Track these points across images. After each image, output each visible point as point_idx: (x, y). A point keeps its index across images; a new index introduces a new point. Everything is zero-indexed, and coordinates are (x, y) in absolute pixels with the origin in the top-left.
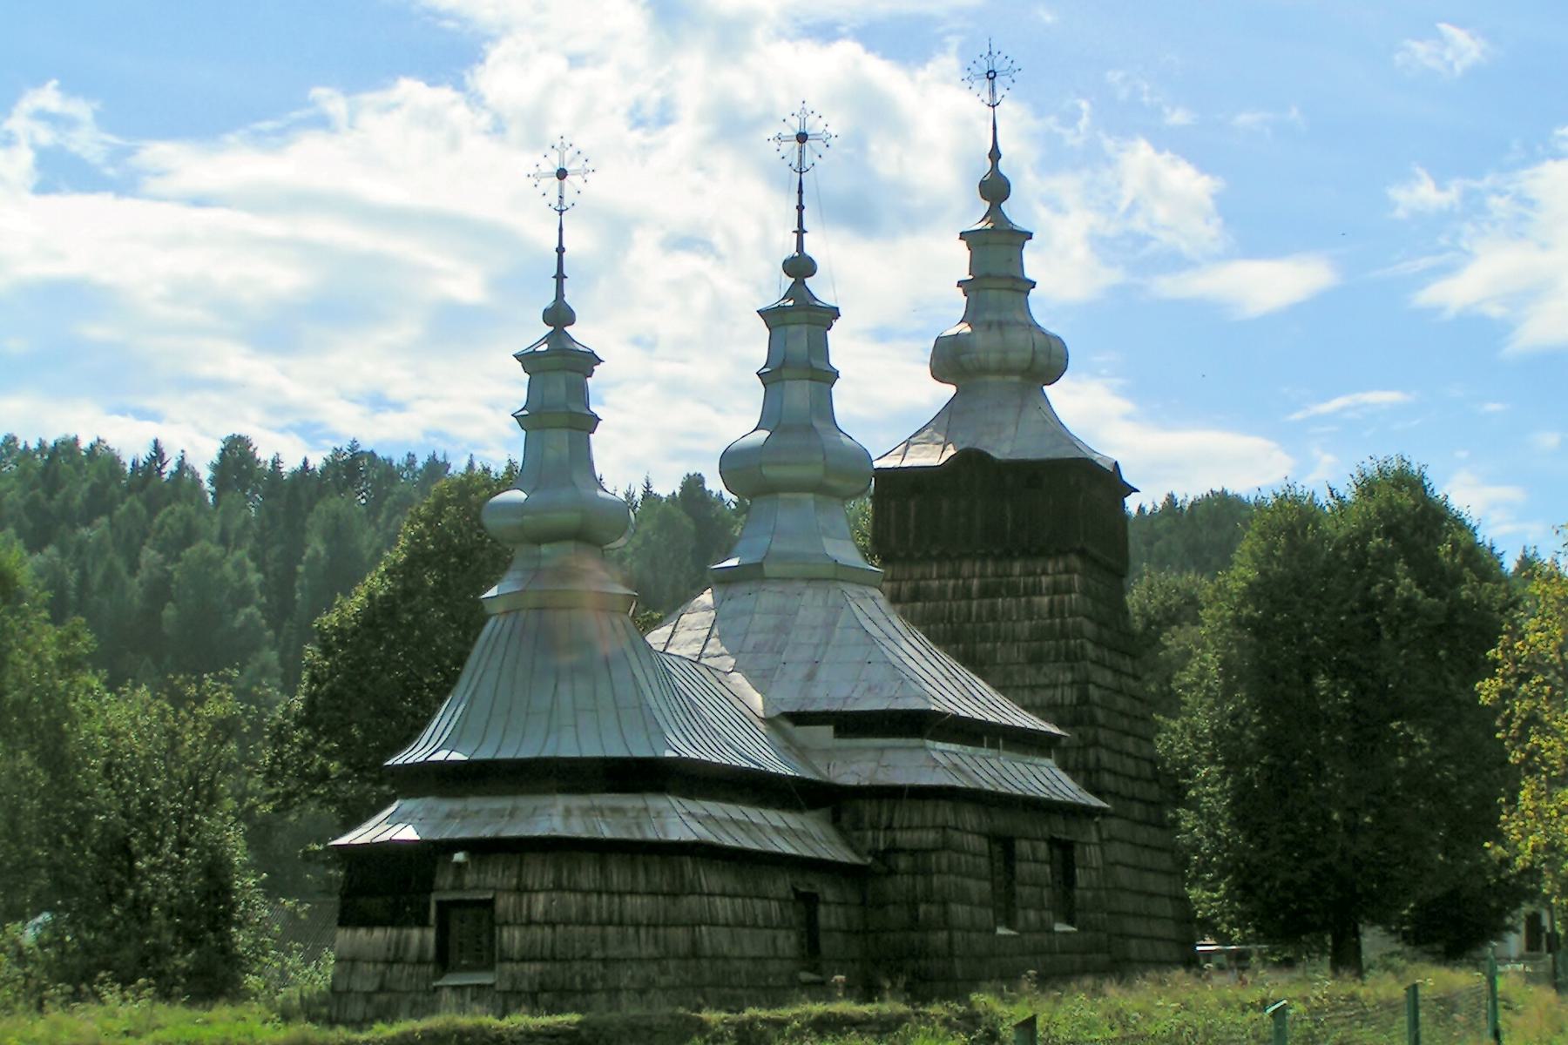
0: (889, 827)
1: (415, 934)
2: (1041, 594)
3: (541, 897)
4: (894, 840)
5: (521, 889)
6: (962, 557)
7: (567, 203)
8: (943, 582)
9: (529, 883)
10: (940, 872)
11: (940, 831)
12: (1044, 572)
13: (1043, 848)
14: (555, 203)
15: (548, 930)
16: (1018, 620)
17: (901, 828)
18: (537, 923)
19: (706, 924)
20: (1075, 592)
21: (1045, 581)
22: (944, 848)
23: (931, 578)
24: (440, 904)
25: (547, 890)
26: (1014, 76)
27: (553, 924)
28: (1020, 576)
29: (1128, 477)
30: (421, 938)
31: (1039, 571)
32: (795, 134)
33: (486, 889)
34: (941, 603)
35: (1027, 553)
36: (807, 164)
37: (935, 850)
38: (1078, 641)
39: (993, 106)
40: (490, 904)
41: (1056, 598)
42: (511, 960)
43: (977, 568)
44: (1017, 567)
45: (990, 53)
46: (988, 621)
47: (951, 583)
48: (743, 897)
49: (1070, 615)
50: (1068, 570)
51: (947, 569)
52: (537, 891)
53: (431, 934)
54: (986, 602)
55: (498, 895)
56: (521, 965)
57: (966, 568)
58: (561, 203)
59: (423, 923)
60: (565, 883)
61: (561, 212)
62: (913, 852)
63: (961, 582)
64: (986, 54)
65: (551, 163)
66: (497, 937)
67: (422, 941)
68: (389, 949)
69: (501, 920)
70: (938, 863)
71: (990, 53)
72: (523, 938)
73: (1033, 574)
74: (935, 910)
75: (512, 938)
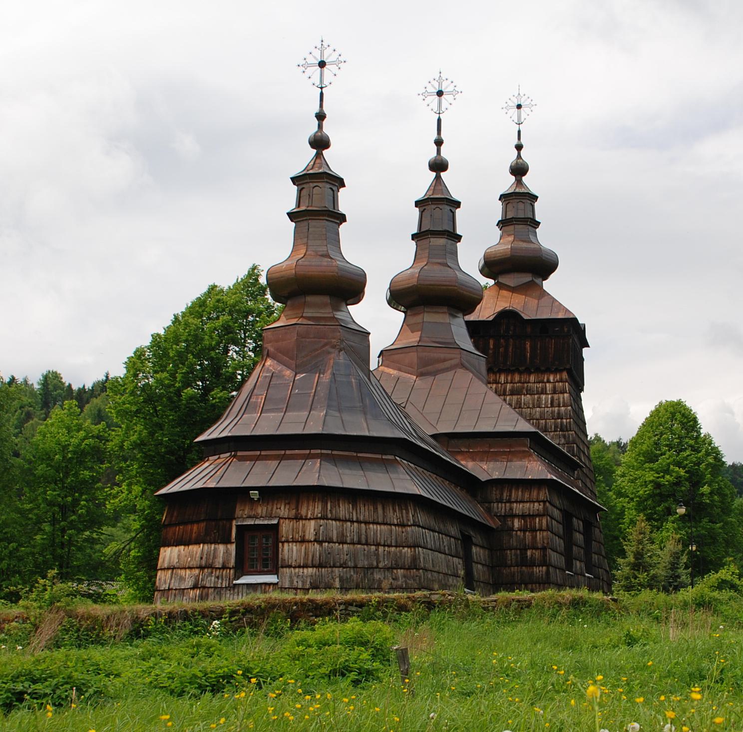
0: (510, 501)
1: (221, 548)
2: (546, 394)
3: (313, 522)
4: (511, 509)
5: (298, 518)
9: (303, 512)
10: (541, 530)
11: (542, 504)
12: (548, 381)
15: (317, 546)
16: (534, 407)
17: (516, 502)
19: (421, 547)
20: (566, 393)
22: (543, 515)
24: (237, 526)
26: (532, 108)
27: (320, 543)
28: (534, 383)
29: (589, 336)
30: (225, 552)
31: (545, 380)
32: (436, 91)
33: (271, 517)
35: (538, 370)
36: (443, 109)
38: (568, 420)
39: (519, 124)
40: (276, 527)
41: (556, 396)
42: (290, 566)
43: (509, 378)
44: (532, 378)
48: (439, 533)
49: (563, 406)
50: (561, 381)
52: (310, 519)
53: (233, 548)
54: (515, 397)
55: (282, 521)
56: (297, 570)
57: (502, 379)
59: (226, 541)
60: (329, 516)
62: (523, 516)
63: (500, 385)
66: (280, 550)
67: (227, 552)
68: (201, 558)
69: (283, 539)
72: (299, 551)
73: (543, 382)
74: (537, 553)
75: (290, 551)
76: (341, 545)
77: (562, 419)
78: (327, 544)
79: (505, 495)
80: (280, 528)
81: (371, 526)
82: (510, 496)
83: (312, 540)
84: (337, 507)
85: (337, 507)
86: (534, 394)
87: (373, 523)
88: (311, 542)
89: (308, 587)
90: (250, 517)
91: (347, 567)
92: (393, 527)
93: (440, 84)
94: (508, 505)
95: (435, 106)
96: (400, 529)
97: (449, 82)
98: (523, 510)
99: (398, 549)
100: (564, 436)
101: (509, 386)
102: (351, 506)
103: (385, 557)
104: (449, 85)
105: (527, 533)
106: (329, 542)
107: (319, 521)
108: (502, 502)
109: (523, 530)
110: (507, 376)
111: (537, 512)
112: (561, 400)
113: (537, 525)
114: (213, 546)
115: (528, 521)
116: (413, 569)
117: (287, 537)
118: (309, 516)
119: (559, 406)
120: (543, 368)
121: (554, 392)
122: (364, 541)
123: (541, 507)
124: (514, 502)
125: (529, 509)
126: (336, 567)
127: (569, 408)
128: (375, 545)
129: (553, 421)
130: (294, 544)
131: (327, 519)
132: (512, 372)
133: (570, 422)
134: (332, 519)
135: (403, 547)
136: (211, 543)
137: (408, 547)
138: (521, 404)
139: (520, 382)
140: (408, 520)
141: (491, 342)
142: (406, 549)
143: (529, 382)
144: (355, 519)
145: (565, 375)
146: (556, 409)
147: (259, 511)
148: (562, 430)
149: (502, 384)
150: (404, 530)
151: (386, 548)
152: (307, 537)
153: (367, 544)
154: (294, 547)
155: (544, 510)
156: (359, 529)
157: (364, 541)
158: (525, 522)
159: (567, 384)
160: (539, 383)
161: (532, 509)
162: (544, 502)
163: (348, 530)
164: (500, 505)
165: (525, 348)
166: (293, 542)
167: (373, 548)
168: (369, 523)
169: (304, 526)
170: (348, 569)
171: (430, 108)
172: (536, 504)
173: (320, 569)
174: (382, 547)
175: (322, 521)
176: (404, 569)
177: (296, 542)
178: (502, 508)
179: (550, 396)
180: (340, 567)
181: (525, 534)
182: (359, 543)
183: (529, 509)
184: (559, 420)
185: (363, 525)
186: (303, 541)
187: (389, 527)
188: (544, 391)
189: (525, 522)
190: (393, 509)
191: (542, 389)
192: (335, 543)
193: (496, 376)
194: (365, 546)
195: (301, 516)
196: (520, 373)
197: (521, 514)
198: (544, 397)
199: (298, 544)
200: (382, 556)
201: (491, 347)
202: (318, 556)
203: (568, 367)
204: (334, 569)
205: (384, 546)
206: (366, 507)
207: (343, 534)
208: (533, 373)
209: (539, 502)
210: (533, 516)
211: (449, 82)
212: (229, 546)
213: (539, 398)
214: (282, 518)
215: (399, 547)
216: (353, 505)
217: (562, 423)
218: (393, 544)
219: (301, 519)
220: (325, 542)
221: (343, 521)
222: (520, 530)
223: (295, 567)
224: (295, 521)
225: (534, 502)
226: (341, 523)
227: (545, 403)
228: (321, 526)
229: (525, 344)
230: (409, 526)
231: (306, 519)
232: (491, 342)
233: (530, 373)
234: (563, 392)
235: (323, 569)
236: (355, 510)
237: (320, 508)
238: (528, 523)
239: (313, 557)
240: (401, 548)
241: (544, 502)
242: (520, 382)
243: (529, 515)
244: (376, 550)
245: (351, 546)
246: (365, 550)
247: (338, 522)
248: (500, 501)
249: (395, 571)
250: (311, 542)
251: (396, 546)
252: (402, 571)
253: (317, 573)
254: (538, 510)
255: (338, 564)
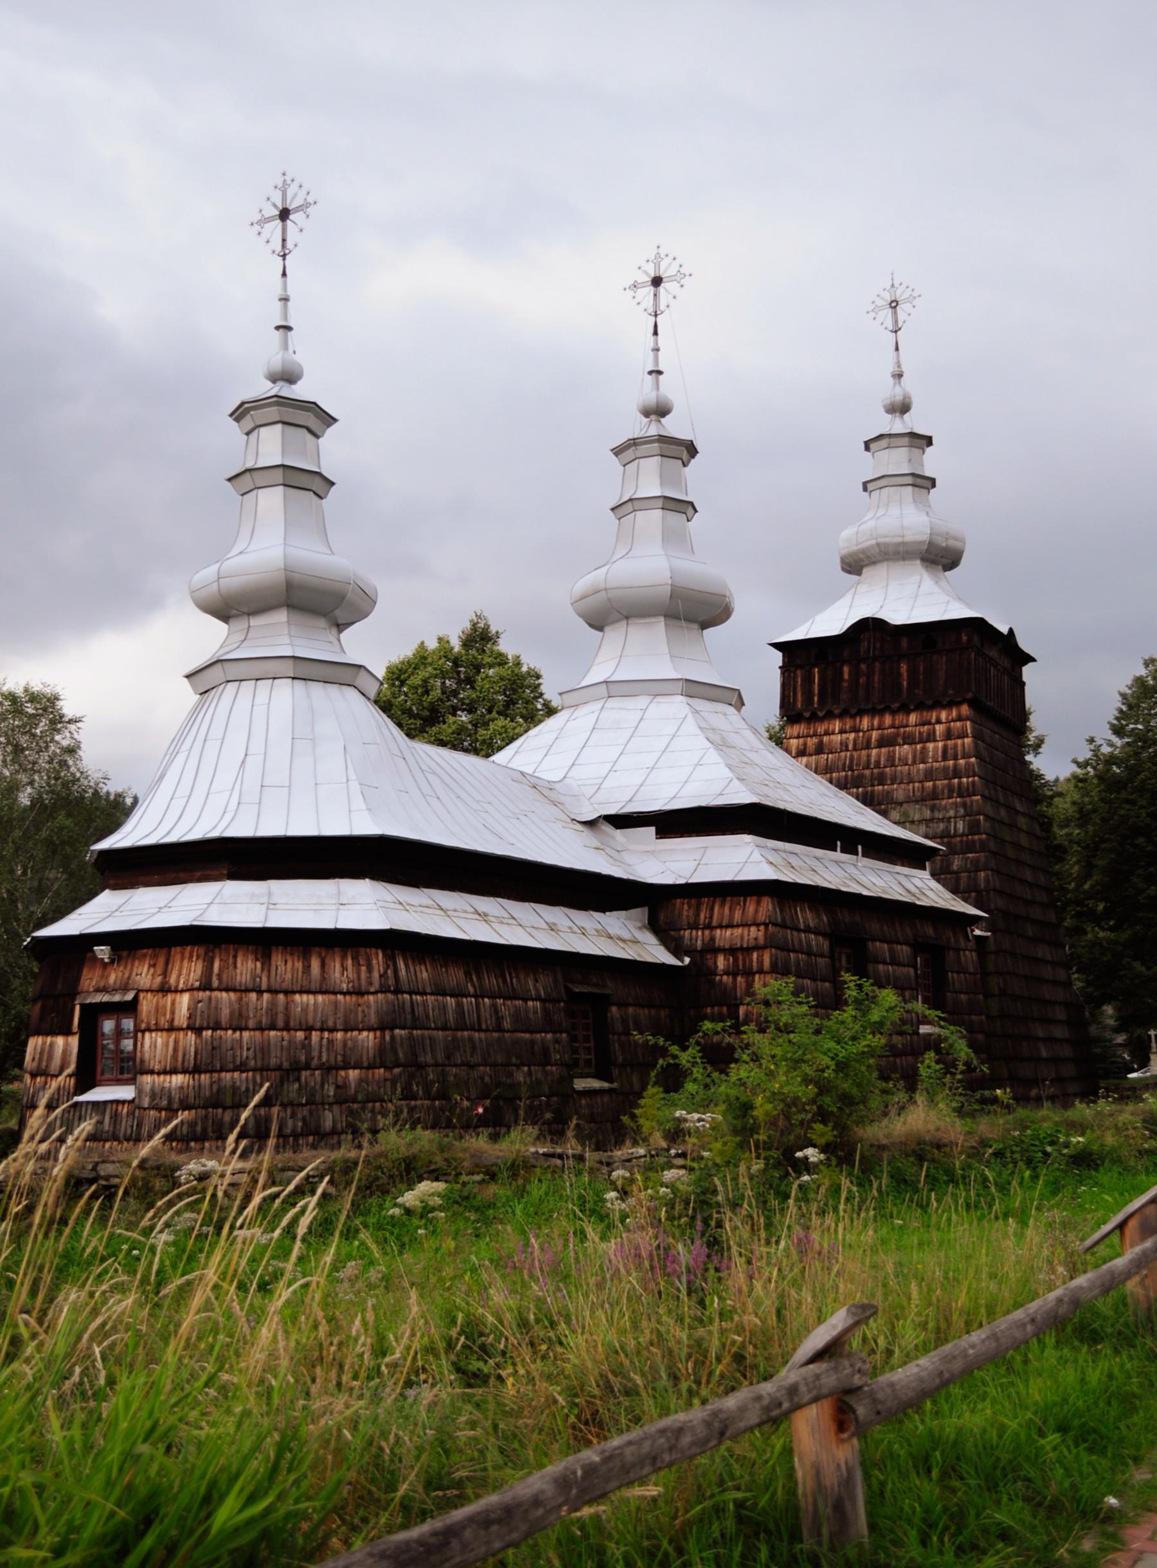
0: (709, 927)
1: (60, 1041)
2: (935, 741)
3: (185, 998)
4: (713, 939)
5: (164, 989)
6: (861, 713)
7: (289, 245)
8: (844, 736)
10: (761, 971)
11: (762, 928)
12: (939, 722)
13: (904, 950)
14: (279, 248)
15: (191, 1036)
16: (914, 763)
17: (721, 927)
18: (181, 1029)
21: (939, 728)
22: (764, 948)
23: (833, 733)
24: (84, 1007)
25: (191, 990)
27: (198, 1031)
31: (933, 720)
32: (649, 279)
34: (843, 754)
35: (920, 707)
36: (662, 307)
37: (757, 948)
42: (152, 1072)
43: (876, 722)
44: (913, 718)
45: (893, 286)
46: (885, 767)
47: (852, 736)
49: (963, 758)
50: (960, 718)
51: (849, 724)
52: (182, 991)
53: (74, 1041)
54: (884, 750)
55: (142, 995)
56: (162, 1077)
57: (865, 723)
58: (284, 246)
59: (67, 1032)
61: (284, 256)
62: (732, 951)
63: (861, 734)
64: (888, 287)
65: (275, 206)
70: (760, 962)
71: (893, 286)
73: (929, 723)
76: (238, 1033)
77: (960, 778)
78: (209, 1032)
79: (702, 916)
80: (139, 1007)
81: (297, 997)
82: (711, 917)
83: (185, 1026)
84: (231, 968)
85: (231, 968)
86: (916, 743)
87: (301, 992)
88: (182, 1029)
89: (175, 1106)
90: (98, 990)
91: (248, 1071)
92: (340, 997)
93: (657, 266)
94: (707, 932)
95: (649, 302)
96: (354, 998)
97: (669, 259)
98: (731, 940)
99: (349, 1034)
100: (964, 805)
101: (875, 735)
102: (259, 964)
103: (324, 1049)
104: (670, 264)
105: (739, 979)
106: (214, 1029)
107: (195, 993)
108: (697, 929)
109: (733, 973)
110: (873, 719)
111: (752, 943)
112: (960, 748)
113: (755, 964)
114: (49, 1039)
115: (741, 957)
116: (379, 1068)
117: (148, 1023)
118: (181, 986)
119: (955, 758)
120: (929, 702)
121: (948, 735)
122: (280, 1023)
123: (761, 934)
124: (716, 928)
125: (742, 937)
126: (227, 1071)
127: (973, 760)
128: (305, 1030)
129: (946, 782)
130: (159, 1034)
131: (212, 990)
132: (881, 712)
133: (973, 782)
134: (220, 990)
135: (360, 1030)
136: (47, 1034)
137: (369, 1030)
138: (894, 760)
139: (893, 726)
140: (371, 984)
141: (846, 669)
142: (365, 1034)
143: (907, 726)
144: (264, 987)
145: (965, 709)
146: (951, 762)
147: (112, 978)
148: (960, 795)
149: (864, 732)
150: (361, 1001)
151: (326, 1034)
152: (176, 1023)
153: (287, 1028)
154: (159, 1040)
155: (766, 939)
156: (273, 1005)
157: (280, 1023)
158: (736, 960)
159: (968, 723)
160: (923, 724)
161: (746, 938)
162: (766, 925)
163: (251, 1007)
164: (694, 932)
165: (899, 675)
166: (157, 1030)
167: (300, 1035)
168: (294, 992)
169: (173, 1003)
170: (250, 1074)
171: (642, 307)
172: (753, 929)
173: (196, 1076)
174: (318, 1033)
175: (201, 994)
176: (361, 1068)
177: (162, 1030)
178: (699, 938)
179: (940, 744)
180: (233, 1071)
181: (735, 980)
182: (273, 1027)
183: (742, 937)
184: (956, 780)
185: (281, 997)
186: (171, 1029)
187: (332, 997)
188: (931, 737)
189: (736, 960)
190: (342, 966)
191: (929, 734)
192: (226, 1029)
193: (855, 721)
194: (285, 1033)
195: (170, 987)
196: (894, 713)
197: (727, 946)
198: (931, 746)
199: (164, 1034)
200: (317, 1047)
201: (846, 676)
202: (193, 1054)
203: (970, 696)
204: (223, 1074)
205: (322, 1030)
206: (289, 964)
207: (240, 1014)
208: (913, 710)
209: (758, 925)
210: (748, 950)
211: (669, 259)
212: (70, 1039)
213: (924, 748)
214: (142, 991)
215: (352, 1030)
216: (263, 964)
217: (960, 784)
218: (338, 1027)
219: (169, 991)
220: (208, 1028)
221: (241, 991)
222: (727, 972)
223: (159, 1074)
224: (160, 995)
225: (750, 926)
226: (238, 994)
227: (933, 756)
228: (200, 1002)
229: (899, 668)
230: (372, 993)
231: (176, 991)
232: (846, 669)
233: (908, 712)
234: (963, 735)
235: (203, 1076)
236: (265, 972)
237: (199, 972)
238: (741, 963)
239: (184, 1055)
240: (355, 1033)
241: (766, 925)
242: (893, 726)
243: (742, 949)
244: (306, 1038)
245: (258, 1033)
246: (283, 1040)
247: (232, 995)
248: (694, 926)
249: (343, 1073)
250: (182, 1029)
251: (346, 1030)
252: (357, 1072)
253: (191, 1082)
254: (756, 939)
255: (231, 1066)
